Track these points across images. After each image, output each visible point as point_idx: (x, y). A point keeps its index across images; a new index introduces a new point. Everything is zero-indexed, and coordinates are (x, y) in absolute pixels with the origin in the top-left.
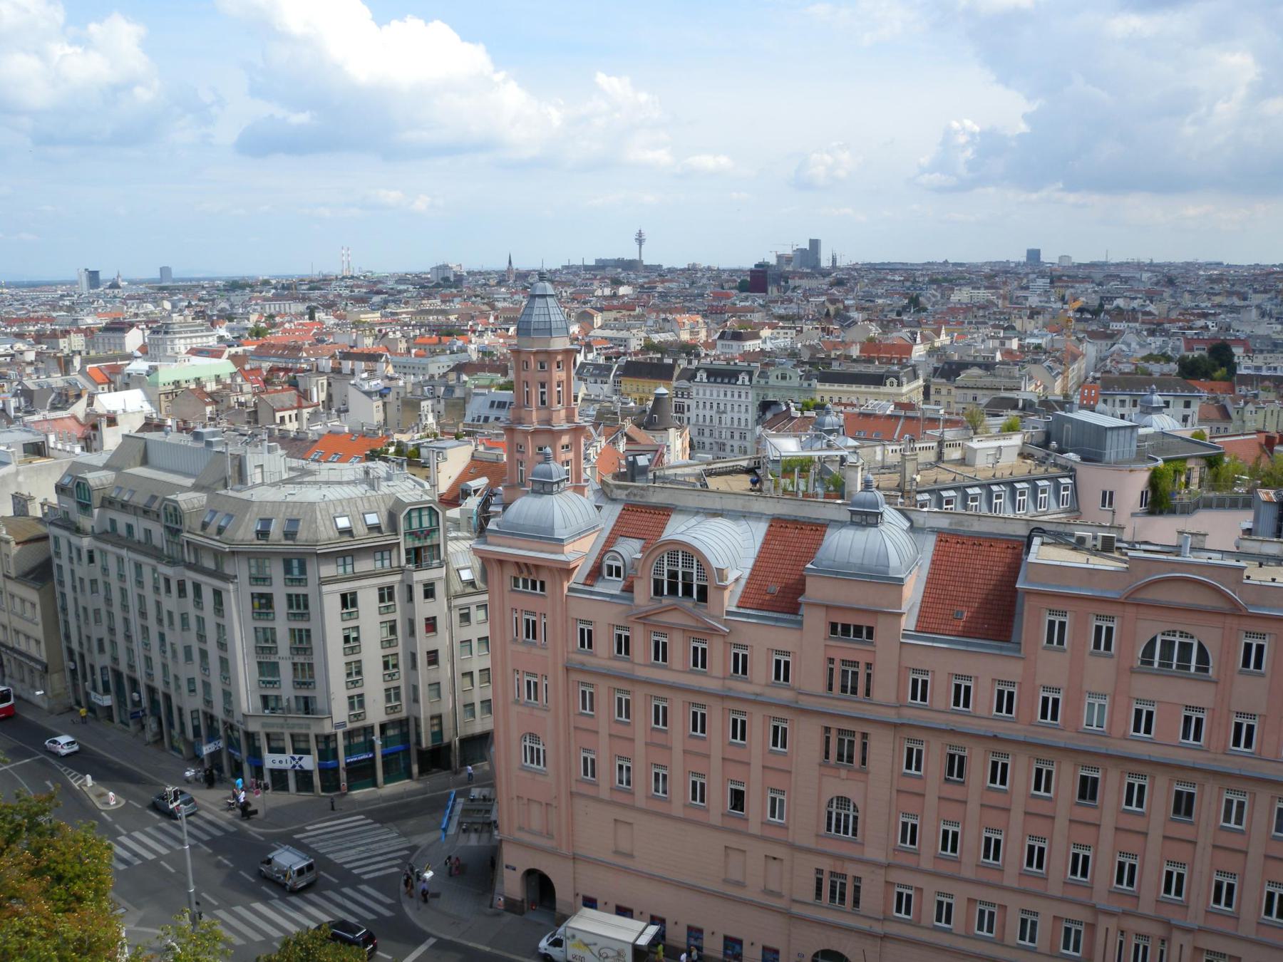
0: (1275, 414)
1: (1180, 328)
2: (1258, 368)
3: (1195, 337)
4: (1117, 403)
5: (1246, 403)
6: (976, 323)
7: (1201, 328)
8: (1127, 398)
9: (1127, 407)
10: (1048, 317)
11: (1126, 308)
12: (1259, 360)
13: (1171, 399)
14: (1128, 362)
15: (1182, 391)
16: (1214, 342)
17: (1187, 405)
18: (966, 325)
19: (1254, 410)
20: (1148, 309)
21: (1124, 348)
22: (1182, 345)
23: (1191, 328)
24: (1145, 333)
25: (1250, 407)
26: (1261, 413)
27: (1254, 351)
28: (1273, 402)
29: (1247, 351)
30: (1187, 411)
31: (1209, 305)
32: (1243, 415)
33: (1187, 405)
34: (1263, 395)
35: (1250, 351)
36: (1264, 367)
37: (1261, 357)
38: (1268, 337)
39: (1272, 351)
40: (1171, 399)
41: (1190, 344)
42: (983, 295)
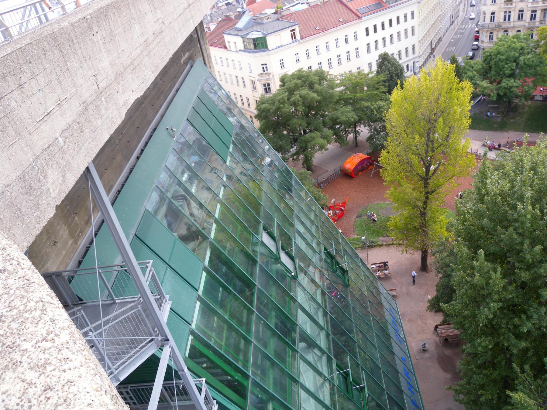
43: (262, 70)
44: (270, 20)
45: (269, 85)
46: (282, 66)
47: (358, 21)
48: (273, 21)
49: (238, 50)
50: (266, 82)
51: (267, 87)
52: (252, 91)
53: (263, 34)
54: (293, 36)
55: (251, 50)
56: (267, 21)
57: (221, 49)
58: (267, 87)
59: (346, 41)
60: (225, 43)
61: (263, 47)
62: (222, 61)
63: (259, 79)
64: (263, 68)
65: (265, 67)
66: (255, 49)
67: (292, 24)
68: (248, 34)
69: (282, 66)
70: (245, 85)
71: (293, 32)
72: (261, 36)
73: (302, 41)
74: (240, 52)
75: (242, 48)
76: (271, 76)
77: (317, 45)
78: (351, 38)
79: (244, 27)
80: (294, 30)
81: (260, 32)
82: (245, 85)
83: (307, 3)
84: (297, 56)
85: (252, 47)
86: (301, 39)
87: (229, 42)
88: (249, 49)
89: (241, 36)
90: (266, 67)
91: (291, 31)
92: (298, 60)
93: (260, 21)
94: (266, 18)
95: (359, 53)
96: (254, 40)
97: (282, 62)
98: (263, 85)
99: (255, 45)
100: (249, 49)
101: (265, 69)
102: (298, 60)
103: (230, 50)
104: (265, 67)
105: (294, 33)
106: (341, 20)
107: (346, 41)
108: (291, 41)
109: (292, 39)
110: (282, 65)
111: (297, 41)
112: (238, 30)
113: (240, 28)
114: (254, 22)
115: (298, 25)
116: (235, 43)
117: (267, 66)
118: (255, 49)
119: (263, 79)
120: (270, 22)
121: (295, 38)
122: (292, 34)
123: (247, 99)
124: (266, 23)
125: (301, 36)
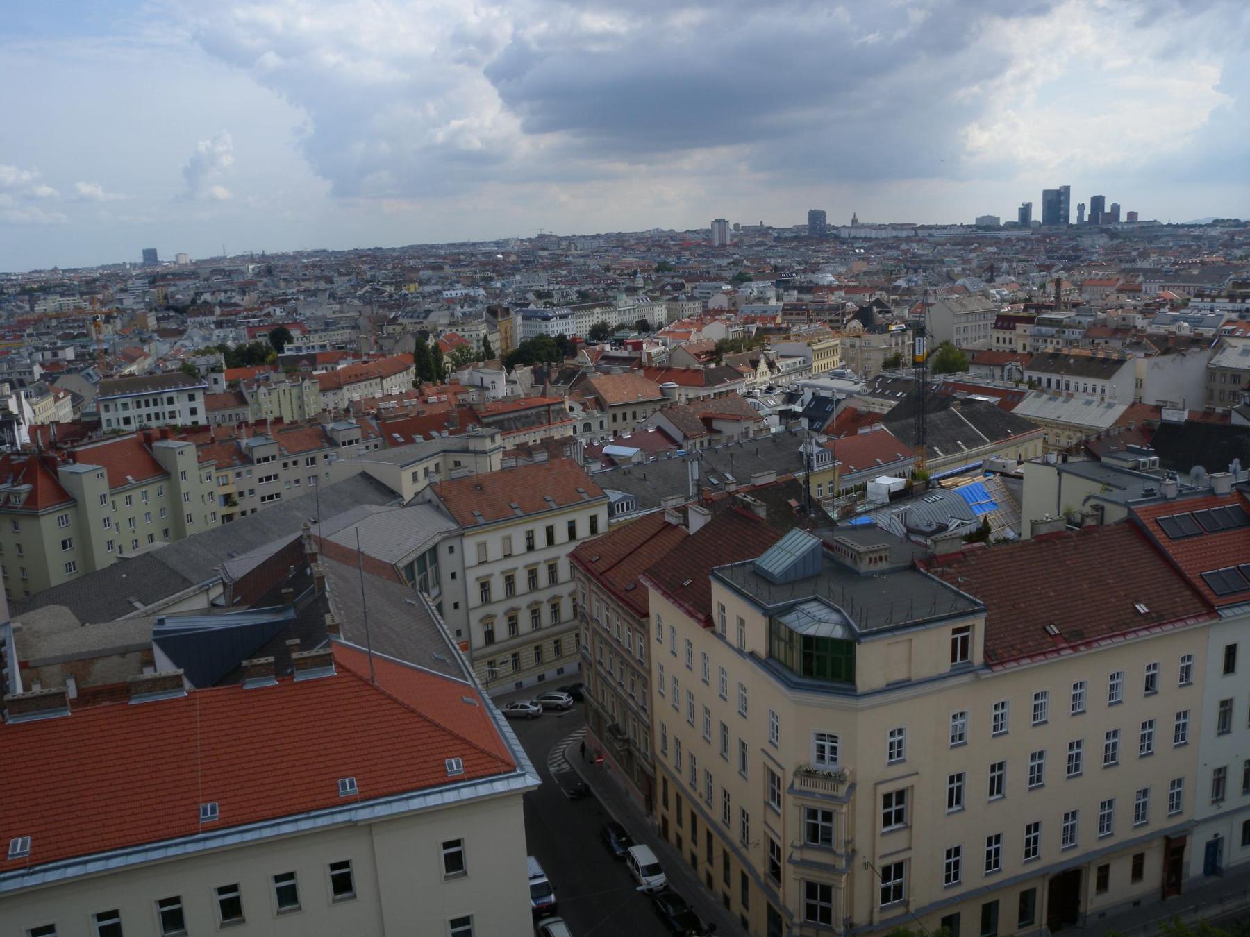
0: (287, 392)
1: (245, 317)
2: (299, 349)
3: (256, 325)
4: (120, 406)
5: (259, 387)
6: (38, 335)
7: (264, 315)
8: (129, 401)
9: (131, 410)
10: (126, 319)
11: (214, 301)
12: (316, 340)
13: (174, 395)
14: (175, 359)
15: (184, 386)
16: (273, 328)
17: (192, 398)
18: (25, 338)
19: (267, 392)
20: (233, 301)
21: (187, 343)
22: (244, 332)
23: (255, 317)
24: (213, 326)
25: (263, 390)
26: (274, 394)
27: (309, 332)
28: (284, 382)
29: (304, 332)
30: (192, 404)
31: (295, 291)
32: (257, 398)
33: (192, 398)
34: (274, 376)
35: (306, 333)
36: (304, 347)
37: (316, 336)
38: (324, 317)
39: (325, 330)
40: (174, 395)
41: (252, 331)
42: (71, 302)
43: (814, 754)
44: (884, 565)
45: (828, 816)
46: (896, 751)
47: (1204, 622)
48: (894, 571)
49: (748, 649)
50: (821, 806)
51: (819, 822)
52: (766, 804)
53: (847, 625)
54: (960, 649)
55: (791, 670)
56: (872, 568)
57: (692, 622)
58: (819, 822)
59: (1150, 683)
60: (711, 607)
61: (836, 676)
62: (690, 654)
63: (797, 786)
64: (821, 748)
65: (827, 746)
66: (808, 671)
67: (962, 606)
68: (790, 608)
69: (896, 751)
70: (744, 766)
71: (959, 636)
72: (838, 633)
73: (986, 674)
74: (749, 663)
75: (762, 649)
76: (843, 789)
77: (1038, 691)
78: (1168, 678)
79: (786, 573)
80: (966, 629)
81: (838, 611)
82: (744, 766)
83: (1003, 474)
84: (959, 721)
85: (796, 660)
86: (988, 665)
87: (723, 609)
88: (785, 665)
89: (766, 612)
90: (834, 750)
91: (956, 631)
92: (959, 738)
93: (848, 562)
94: (871, 555)
95: (1189, 732)
96: (809, 641)
97: (897, 738)
98: (804, 814)
99: (807, 657)
100: (785, 665)
101: (827, 754)
102: (959, 738)
103: (722, 637)
104: (827, 746)
105: (965, 640)
106: (1142, 608)
107: (1150, 683)
108: (946, 666)
109: (954, 659)
110: (895, 750)
111: (967, 669)
112: (763, 577)
113: (771, 574)
114: (825, 556)
115: (985, 615)
116: (742, 622)
117: (839, 745)
118: (808, 671)
119: (812, 794)
120: (882, 573)
121: (964, 655)
122: (954, 641)
123: (744, 814)
124: (869, 577)
125: (988, 654)
